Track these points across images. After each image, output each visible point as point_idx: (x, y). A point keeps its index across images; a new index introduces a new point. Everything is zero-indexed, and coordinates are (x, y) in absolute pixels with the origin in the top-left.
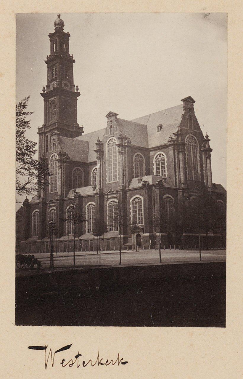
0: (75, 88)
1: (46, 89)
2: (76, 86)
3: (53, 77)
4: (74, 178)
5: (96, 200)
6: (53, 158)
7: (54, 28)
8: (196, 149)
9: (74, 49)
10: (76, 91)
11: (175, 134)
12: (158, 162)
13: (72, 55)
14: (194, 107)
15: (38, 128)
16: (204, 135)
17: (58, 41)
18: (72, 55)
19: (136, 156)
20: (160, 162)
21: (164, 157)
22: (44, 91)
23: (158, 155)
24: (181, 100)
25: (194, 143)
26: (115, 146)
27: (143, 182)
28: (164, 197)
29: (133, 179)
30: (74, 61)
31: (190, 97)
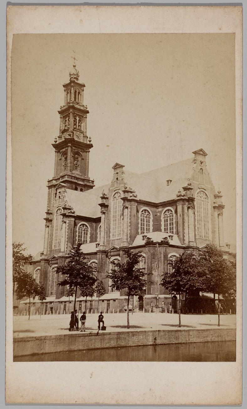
0: (88, 139)
4: (79, 233)
5: (98, 258)
6: (59, 212)
8: (208, 204)
10: (88, 143)
12: (166, 218)
13: (86, 106)
15: (48, 180)
18: (86, 106)
20: (169, 218)
21: (172, 212)
22: (56, 142)
23: (166, 211)
24: (193, 152)
25: (199, 197)
26: (120, 200)
27: (147, 238)
28: (169, 256)
30: (88, 112)
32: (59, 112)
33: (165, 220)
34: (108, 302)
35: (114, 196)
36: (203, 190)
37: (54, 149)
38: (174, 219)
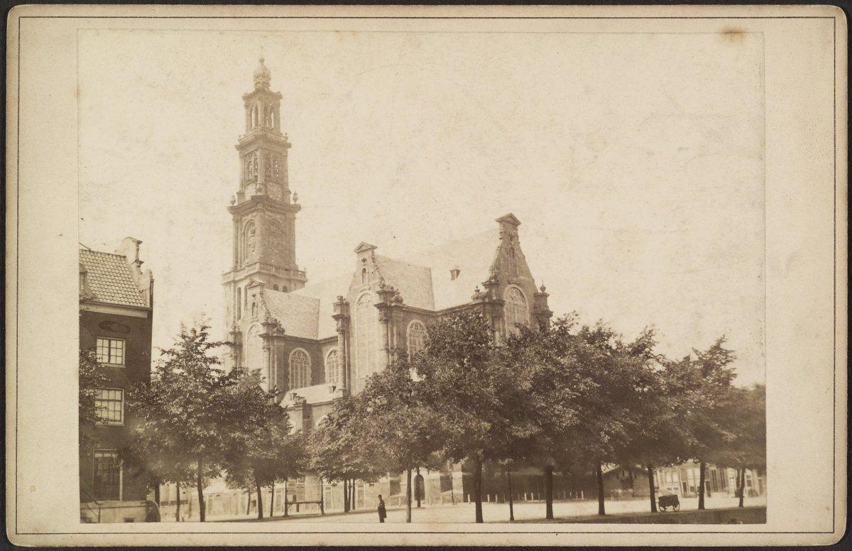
0: (292, 196)
1: (236, 197)
2: (293, 193)
3: (250, 177)
6: (254, 330)
9: (291, 124)
10: (292, 202)
11: (485, 285)
13: (286, 134)
15: (222, 273)
16: (538, 285)
17: (259, 108)
18: (286, 134)
19: (413, 325)
30: (289, 146)
31: (511, 216)
35: (359, 300)
37: (231, 216)
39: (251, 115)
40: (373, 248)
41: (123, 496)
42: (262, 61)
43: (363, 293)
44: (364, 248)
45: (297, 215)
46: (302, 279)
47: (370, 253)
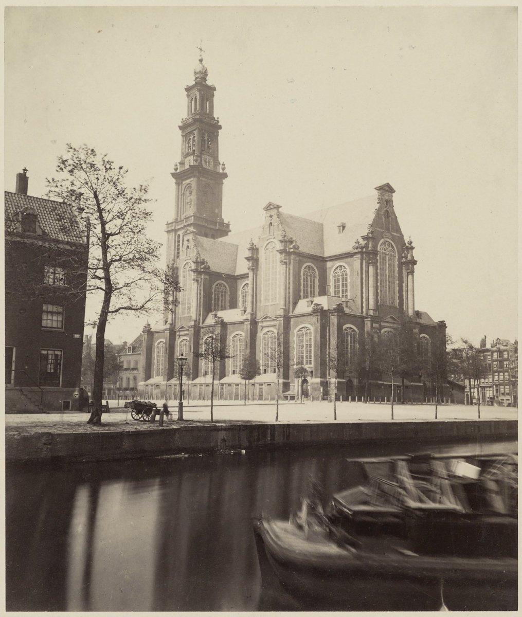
0: (221, 166)
1: (178, 166)
3: (190, 150)
6: (187, 267)
7: (194, 78)
9: (221, 110)
10: (221, 171)
11: (364, 238)
14: (394, 199)
16: (406, 240)
17: (198, 97)
18: (218, 118)
20: (340, 278)
22: (176, 169)
23: (337, 267)
24: (375, 188)
27: (315, 304)
29: (300, 301)
30: (220, 127)
31: (388, 185)
32: (180, 128)
33: (335, 279)
34: (261, 387)
35: (266, 247)
36: (389, 240)
37: (174, 180)
38: (348, 278)
39: (191, 103)
40: (278, 207)
41: (62, 385)
42: (201, 61)
43: (269, 241)
44: (271, 207)
45: (224, 181)
46: (227, 229)
47: (275, 211)
